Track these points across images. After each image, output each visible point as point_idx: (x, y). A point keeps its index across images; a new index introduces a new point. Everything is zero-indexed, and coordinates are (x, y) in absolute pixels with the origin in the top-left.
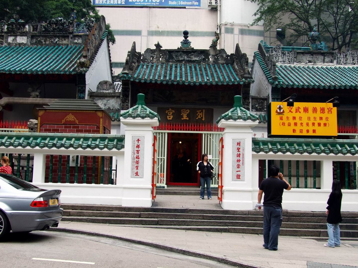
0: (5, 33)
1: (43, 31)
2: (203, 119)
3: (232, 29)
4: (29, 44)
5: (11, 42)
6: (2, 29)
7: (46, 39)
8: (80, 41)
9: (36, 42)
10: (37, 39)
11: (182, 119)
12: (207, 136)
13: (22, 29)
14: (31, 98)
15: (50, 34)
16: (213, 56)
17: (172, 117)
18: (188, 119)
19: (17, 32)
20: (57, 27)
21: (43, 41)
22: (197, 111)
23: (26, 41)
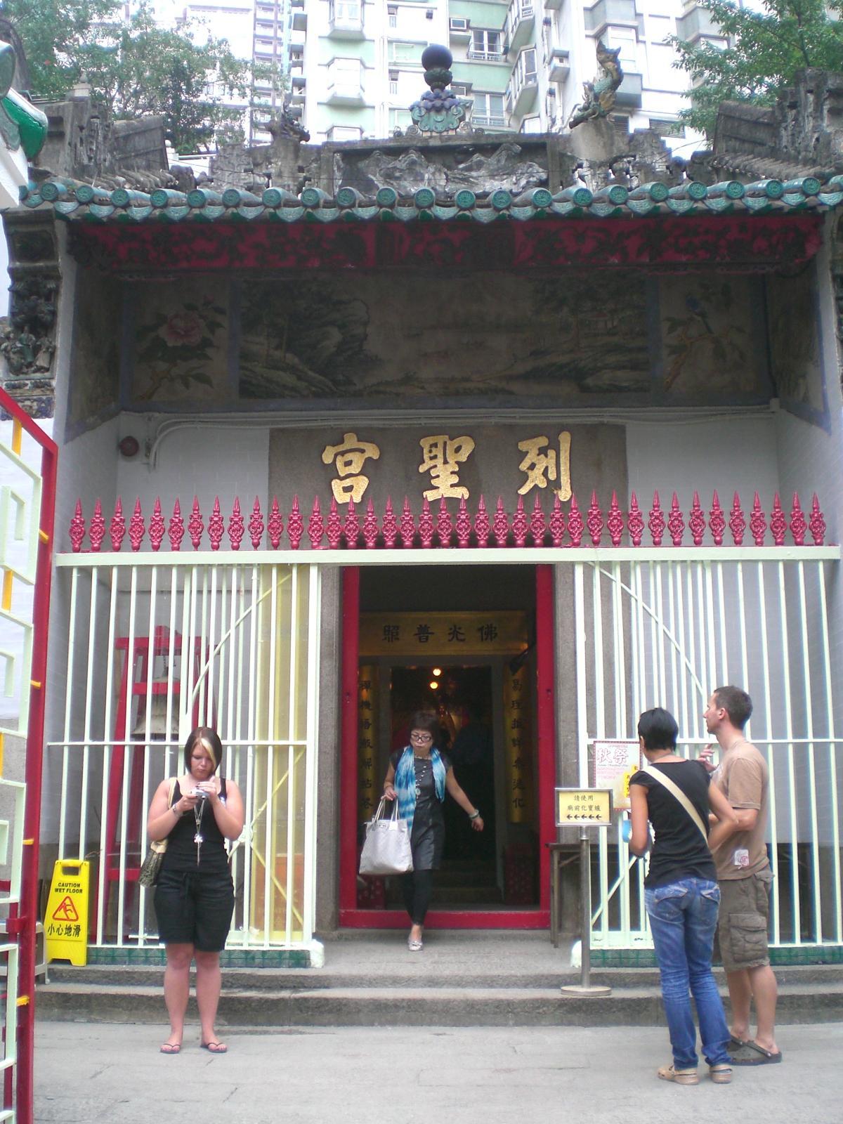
2: (565, 494)
11: (430, 495)
12: (607, 584)
16: (592, 166)
17: (362, 484)
18: (462, 493)
22: (523, 446)
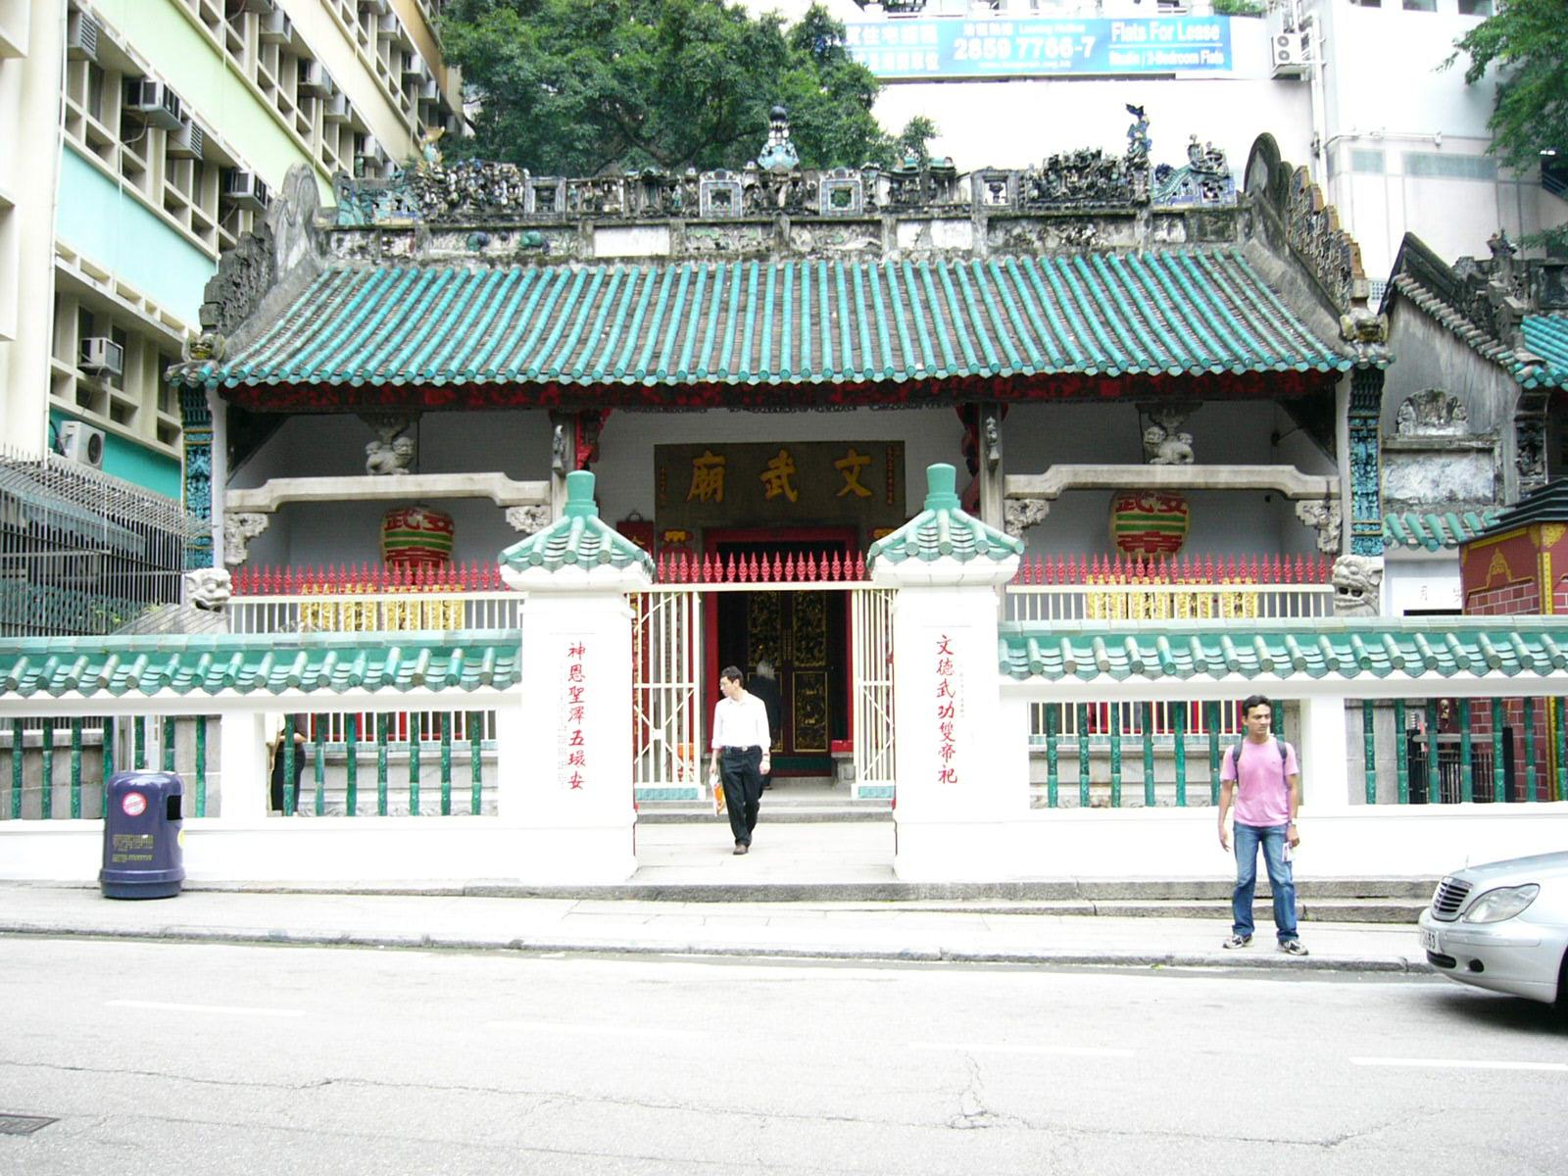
0: (885, 209)
1: (1033, 200)
3: (1379, 156)
4: (984, 251)
5: (911, 246)
6: (872, 197)
7: (1046, 231)
8: (1179, 233)
9: (1006, 244)
10: (1008, 231)
13: (944, 192)
14: (1159, 468)
15: (1058, 208)
19: (930, 207)
20: (1084, 183)
21: (1033, 237)
23: (969, 239)
